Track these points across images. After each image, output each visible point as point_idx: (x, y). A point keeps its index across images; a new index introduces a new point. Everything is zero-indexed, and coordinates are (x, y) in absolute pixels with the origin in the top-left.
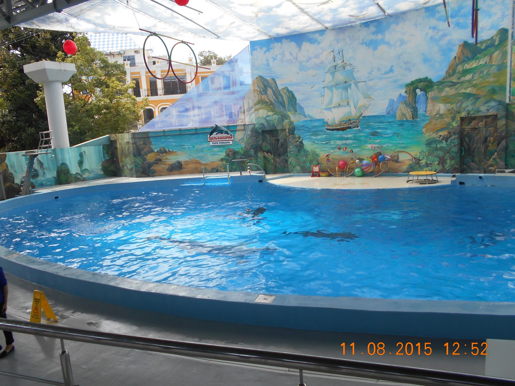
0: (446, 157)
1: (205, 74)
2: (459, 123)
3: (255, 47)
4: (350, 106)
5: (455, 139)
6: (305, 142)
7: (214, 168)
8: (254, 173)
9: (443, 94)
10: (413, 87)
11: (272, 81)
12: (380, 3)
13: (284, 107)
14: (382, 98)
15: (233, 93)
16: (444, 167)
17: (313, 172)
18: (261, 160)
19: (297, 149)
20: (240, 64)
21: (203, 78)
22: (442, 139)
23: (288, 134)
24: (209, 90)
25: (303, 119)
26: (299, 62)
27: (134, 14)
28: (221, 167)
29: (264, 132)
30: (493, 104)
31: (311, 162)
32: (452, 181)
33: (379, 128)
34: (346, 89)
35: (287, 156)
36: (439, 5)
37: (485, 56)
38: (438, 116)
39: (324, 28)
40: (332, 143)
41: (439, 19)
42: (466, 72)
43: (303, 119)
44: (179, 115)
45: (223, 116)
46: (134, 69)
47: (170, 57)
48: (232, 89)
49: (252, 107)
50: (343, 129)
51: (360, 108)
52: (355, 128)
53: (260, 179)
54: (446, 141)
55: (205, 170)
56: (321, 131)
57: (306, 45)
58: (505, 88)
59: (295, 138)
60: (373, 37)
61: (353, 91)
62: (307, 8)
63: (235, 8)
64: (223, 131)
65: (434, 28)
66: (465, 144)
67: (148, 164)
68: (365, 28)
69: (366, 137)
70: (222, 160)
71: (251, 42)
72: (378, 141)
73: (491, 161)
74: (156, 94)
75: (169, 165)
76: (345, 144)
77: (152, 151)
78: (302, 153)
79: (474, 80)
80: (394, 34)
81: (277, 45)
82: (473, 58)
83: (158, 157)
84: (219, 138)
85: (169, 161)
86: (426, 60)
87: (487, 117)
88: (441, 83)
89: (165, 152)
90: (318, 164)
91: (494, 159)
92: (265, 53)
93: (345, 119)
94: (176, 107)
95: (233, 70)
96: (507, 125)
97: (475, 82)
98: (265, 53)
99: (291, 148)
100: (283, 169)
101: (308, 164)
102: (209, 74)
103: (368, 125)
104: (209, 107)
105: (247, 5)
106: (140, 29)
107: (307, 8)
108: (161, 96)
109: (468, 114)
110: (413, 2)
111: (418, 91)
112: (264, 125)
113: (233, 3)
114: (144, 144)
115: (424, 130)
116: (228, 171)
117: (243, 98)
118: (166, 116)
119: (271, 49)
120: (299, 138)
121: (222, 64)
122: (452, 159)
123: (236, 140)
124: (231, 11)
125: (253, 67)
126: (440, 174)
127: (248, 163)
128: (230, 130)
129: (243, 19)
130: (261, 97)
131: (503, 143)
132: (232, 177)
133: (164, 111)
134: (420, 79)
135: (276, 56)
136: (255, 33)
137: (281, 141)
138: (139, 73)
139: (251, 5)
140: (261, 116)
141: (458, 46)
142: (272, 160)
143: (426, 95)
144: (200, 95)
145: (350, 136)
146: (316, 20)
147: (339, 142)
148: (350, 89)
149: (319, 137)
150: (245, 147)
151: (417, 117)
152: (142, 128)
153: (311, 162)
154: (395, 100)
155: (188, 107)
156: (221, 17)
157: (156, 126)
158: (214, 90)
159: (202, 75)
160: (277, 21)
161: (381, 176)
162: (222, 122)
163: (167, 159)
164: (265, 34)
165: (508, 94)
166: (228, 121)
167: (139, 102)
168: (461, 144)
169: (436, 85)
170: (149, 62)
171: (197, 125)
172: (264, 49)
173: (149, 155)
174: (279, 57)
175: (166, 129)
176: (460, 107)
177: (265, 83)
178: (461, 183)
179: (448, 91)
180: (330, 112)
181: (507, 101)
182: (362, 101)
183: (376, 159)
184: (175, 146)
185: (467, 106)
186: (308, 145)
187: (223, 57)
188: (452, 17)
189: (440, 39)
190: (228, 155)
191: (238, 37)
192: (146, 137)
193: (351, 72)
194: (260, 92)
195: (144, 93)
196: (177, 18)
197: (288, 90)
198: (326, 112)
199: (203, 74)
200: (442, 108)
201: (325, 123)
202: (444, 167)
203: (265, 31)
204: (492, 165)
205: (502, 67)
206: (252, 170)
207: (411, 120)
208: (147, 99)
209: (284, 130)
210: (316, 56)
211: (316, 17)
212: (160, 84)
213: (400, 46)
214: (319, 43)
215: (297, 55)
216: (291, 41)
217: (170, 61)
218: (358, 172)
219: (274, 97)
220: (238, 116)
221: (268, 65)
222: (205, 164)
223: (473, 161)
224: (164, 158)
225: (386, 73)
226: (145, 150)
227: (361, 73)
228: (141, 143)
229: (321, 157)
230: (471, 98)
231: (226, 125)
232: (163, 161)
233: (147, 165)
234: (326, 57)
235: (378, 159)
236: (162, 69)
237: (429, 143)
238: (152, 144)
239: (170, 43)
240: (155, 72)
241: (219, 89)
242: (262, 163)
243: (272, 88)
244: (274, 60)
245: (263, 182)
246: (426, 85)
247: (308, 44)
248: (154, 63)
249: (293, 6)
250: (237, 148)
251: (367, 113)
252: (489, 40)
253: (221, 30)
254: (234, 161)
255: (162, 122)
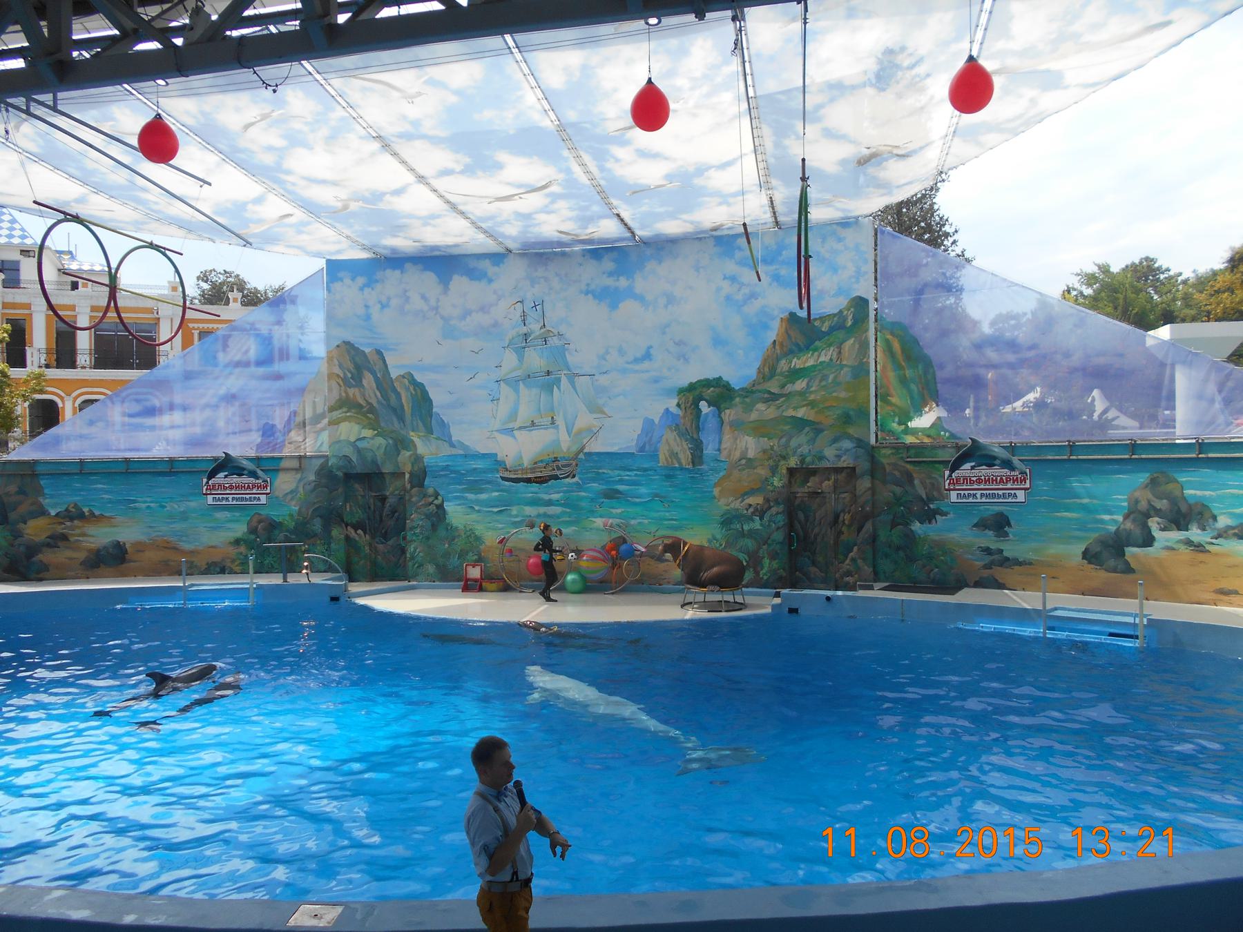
0: (761, 553)
1: (210, 326)
2: (785, 480)
3: (341, 275)
4: (557, 428)
5: (777, 513)
6: (449, 507)
7: (215, 564)
8: (318, 579)
9: (754, 416)
10: (693, 394)
11: (376, 357)
12: (623, 215)
13: (401, 419)
14: (628, 417)
15: (278, 377)
16: (757, 573)
17: (467, 580)
18: (338, 547)
19: (429, 524)
20: (302, 311)
21: (204, 334)
22: (753, 513)
23: (408, 486)
24: (216, 365)
25: (446, 450)
26: (442, 318)
27: (22, 164)
28: (233, 561)
29: (349, 477)
30: (847, 444)
31: (462, 554)
32: (774, 607)
33: (621, 482)
34: (549, 388)
35: (404, 538)
36: (737, 236)
37: (830, 346)
38: (743, 462)
39: (501, 250)
40: (514, 512)
41: (741, 263)
42: (795, 374)
43: (446, 450)
44: (130, 425)
45: (250, 430)
46: (14, 296)
47: (113, 278)
48: (278, 367)
49: (322, 416)
50: (541, 481)
51: (579, 432)
52: (568, 480)
53: (333, 595)
54: (761, 518)
55: (190, 568)
56: (489, 482)
57: (459, 283)
58: (868, 415)
59: (425, 496)
60: (610, 282)
61: (564, 395)
62: (465, 204)
63: (294, 184)
64: (244, 469)
65: (733, 279)
66: (798, 526)
67: (28, 547)
68: (594, 262)
69: (592, 500)
70: (237, 542)
71: (328, 262)
72: (619, 511)
73: (847, 565)
74: (72, 364)
75: (90, 551)
76: (545, 515)
77: (43, 512)
78: (442, 532)
79: (811, 393)
80: (653, 280)
81: (393, 275)
82: (807, 348)
83: (60, 529)
84: (231, 487)
85: (91, 539)
86: (718, 341)
87: (838, 470)
88: (747, 392)
89: (81, 516)
90: (479, 560)
91: (853, 560)
92: (361, 289)
93: (546, 458)
94: (123, 402)
95: (279, 323)
96: (873, 490)
97: (812, 397)
98: (361, 289)
99: (416, 519)
100: (394, 571)
101: (454, 561)
102: (220, 326)
103: (598, 473)
104: (217, 406)
105: (323, 182)
106: (35, 202)
107: (465, 204)
108: (85, 369)
109: (802, 461)
110: (692, 223)
111: (703, 405)
112: (350, 461)
113: (289, 172)
114: (22, 492)
115: (716, 492)
116: (251, 570)
117: (302, 391)
118: (91, 423)
119: (377, 281)
120: (436, 495)
121: (255, 304)
122: (773, 556)
123: (277, 493)
124: (284, 189)
125: (331, 319)
126: (750, 589)
127: (304, 552)
128: (263, 468)
129: (313, 210)
130: (346, 392)
131: (868, 526)
132: (260, 587)
133: (89, 409)
134: (707, 380)
135: (389, 299)
136: (339, 243)
137: (391, 501)
138: (28, 306)
139: (335, 184)
140: (342, 438)
141: (779, 320)
142: (367, 548)
143: (719, 416)
144: (188, 376)
145: (555, 497)
146: (485, 232)
147: (530, 511)
148: (559, 388)
149: (484, 496)
150: (300, 513)
151: (701, 463)
152: (21, 451)
153: (462, 554)
154: (657, 421)
155: (157, 403)
156: (259, 200)
157: (64, 446)
158: (226, 366)
159: (201, 326)
160: (395, 224)
161: (624, 591)
162: (242, 447)
163: (84, 535)
164: (364, 248)
165: (873, 424)
166: (259, 446)
167: (17, 381)
168: (790, 526)
169: (740, 396)
170: (59, 283)
171: (177, 452)
172: (361, 280)
173: (32, 524)
174: (394, 302)
175: (90, 454)
176: (786, 446)
177: (357, 359)
178: (793, 611)
179: (763, 411)
180: (511, 439)
181: (873, 441)
182: (585, 419)
183: (614, 553)
184: (110, 501)
185: (800, 446)
186: (456, 513)
187: (261, 288)
188: (765, 261)
189: (745, 302)
190: (253, 530)
191: (298, 248)
192: (29, 472)
193: (562, 351)
194: (345, 380)
195: (36, 359)
196: (144, 190)
197: (414, 380)
198: (501, 438)
199: (206, 326)
200: (750, 445)
201: (499, 464)
202: (757, 573)
203: (365, 242)
204: (849, 574)
205: (860, 371)
206: (314, 569)
207: (691, 466)
208: (39, 377)
209: (398, 475)
210: (483, 309)
211: (483, 225)
212: (84, 341)
213: (666, 307)
214: (490, 281)
215: (438, 300)
216: (426, 269)
217: (113, 288)
218: (574, 581)
219: (378, 394)
220: (290, 431)
221: (368, 317)
222: (192, 552)
223: (814, 563)
224: (78, 531)
225: (636, 361)
226: (23, 509)
227: (582, 356)
228: (13, 488)
229: (488, 543)
230: (807, 429)
231: (252, 454)
232: (72, 539)
233: (22, 549)
234: (505, 313)
235: (618, 552)
236: (95, 303)
237: (728, 520)
238: (44, 495)
239: (117, 246)
240: (73, 308)
241: (238, 364)
242: (341, 555)
243: (373, 373)
244: (383, 307)
245: (342, 600)
246: (717, 393)
247: (465, 279)
248: (75, 286)
249: (433, 196)
250: (277, 514)
251: (596, 447)
252: (835, 315)
253: (256, 229)
254: (269, 545)
255: (81, 437)
